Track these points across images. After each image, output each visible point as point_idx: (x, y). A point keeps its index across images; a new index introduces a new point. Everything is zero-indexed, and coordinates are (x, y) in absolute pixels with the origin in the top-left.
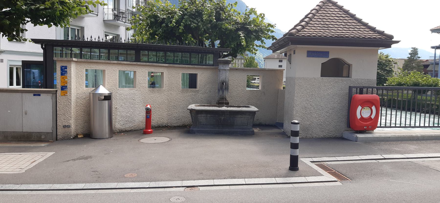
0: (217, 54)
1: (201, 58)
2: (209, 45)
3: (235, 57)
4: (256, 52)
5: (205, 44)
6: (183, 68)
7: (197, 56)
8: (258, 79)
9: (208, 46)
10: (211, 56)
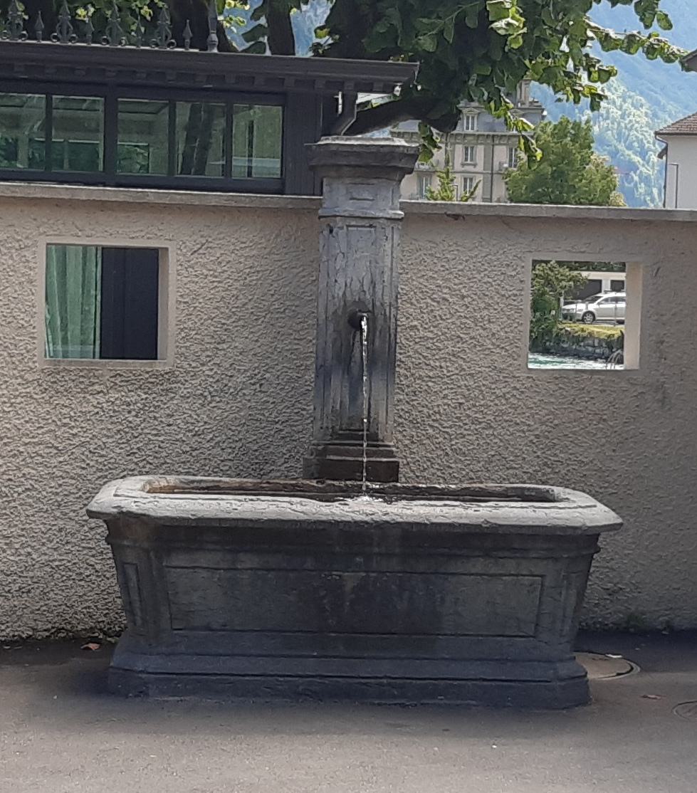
0: (310, 104)
1: (190, 128)
2: (248, 36)
3: (448, 122)
4: (599, 87)
5: (221, 30)
6: (58, 204)
7: (164, 116)
8: (617, 286)
9: (240, 45)
10: (265, 119)
